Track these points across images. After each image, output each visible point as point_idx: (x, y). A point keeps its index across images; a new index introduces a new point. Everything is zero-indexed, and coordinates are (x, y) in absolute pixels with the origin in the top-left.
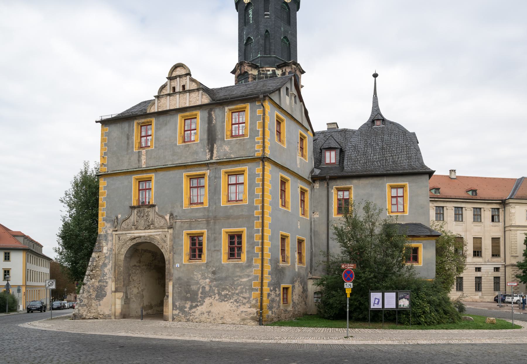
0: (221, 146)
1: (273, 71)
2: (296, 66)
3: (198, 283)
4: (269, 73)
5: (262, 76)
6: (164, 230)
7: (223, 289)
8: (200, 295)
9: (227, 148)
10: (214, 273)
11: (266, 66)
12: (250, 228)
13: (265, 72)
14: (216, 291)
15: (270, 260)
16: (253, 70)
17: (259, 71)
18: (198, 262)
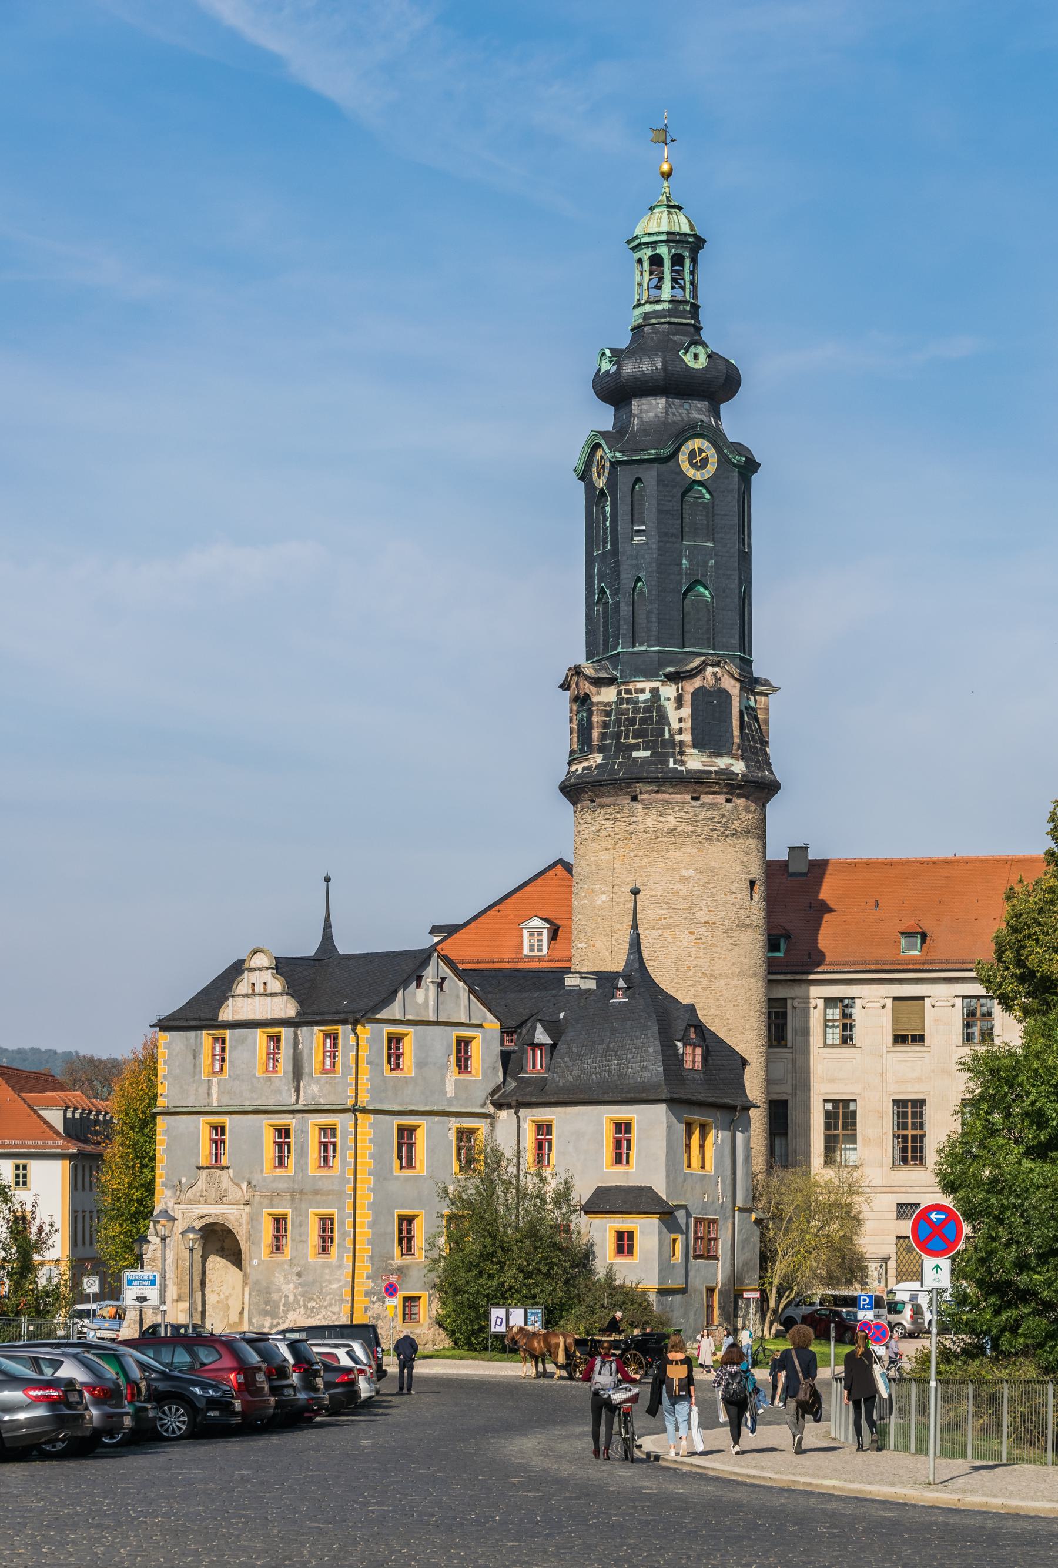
0: (310, 1085)
1: (652, 690)
3: (279, 1290)
4: (642, 697)
5: (624, 706)
6: (238, 1207)
7: (312, 1299)
8: (282, 1308)
9: (315, 1088)
10: (299, 1275)
11: (637, 679)
12: (341, 1209)
13: (634, 695)
14: (302, 1303)
15: (371, 1258)
16: (603, 690)
17: (619, 693)
18: (279, 1258)
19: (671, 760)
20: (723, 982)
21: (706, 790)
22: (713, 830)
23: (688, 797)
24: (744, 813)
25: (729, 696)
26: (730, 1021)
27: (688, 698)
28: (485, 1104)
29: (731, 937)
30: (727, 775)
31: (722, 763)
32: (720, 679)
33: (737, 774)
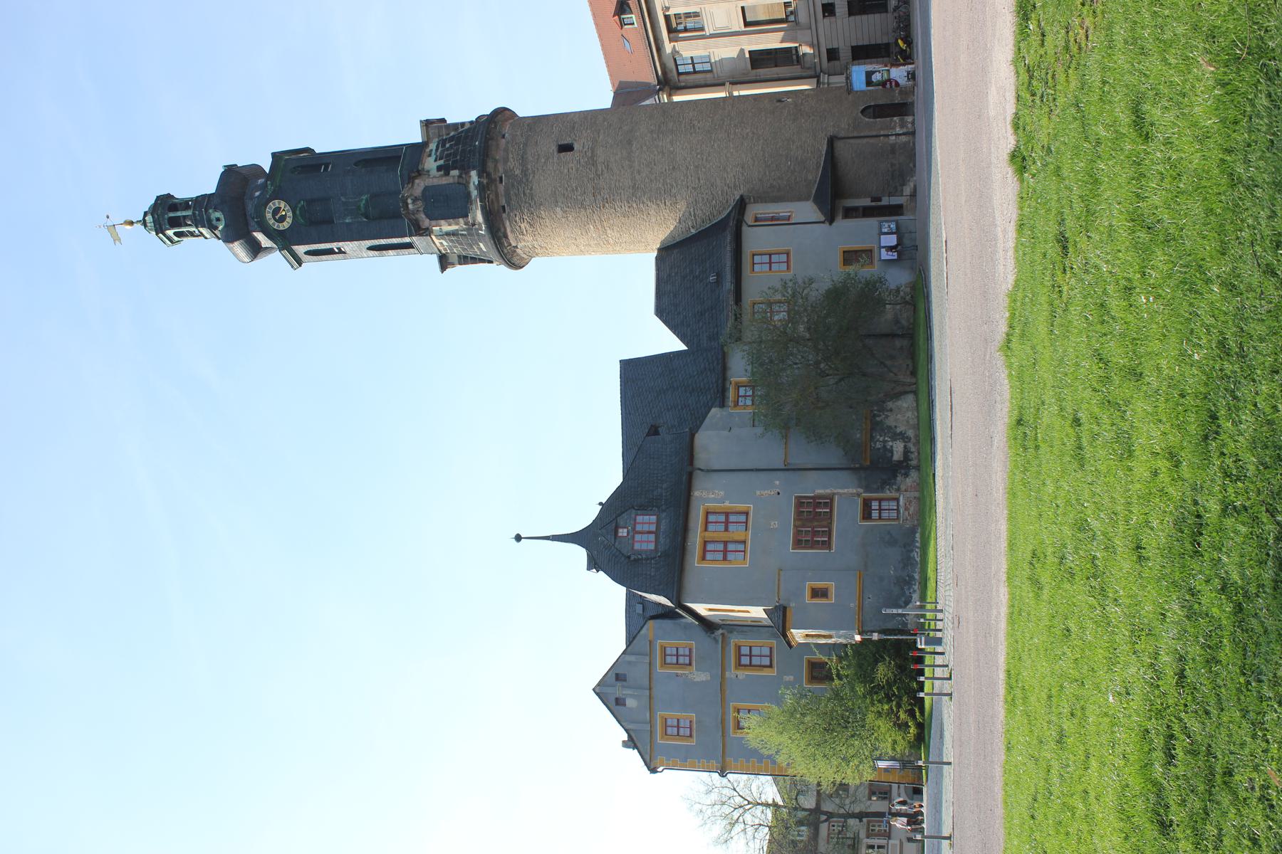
2: (407, 199)
4: (445, 243)
19: (480, 232)
20: (637, 177)
21: (496, 205)
22: (525, 194)
23: (504, 215)
24: (509, 163)
25: (426, 189)
26: (667, 168)
27: (434, 223)
28: (715, 638)
29: (602, 171)
30: (482, 188)
31: (474, 193)
32: (416, 197)
33: (479, 181)
